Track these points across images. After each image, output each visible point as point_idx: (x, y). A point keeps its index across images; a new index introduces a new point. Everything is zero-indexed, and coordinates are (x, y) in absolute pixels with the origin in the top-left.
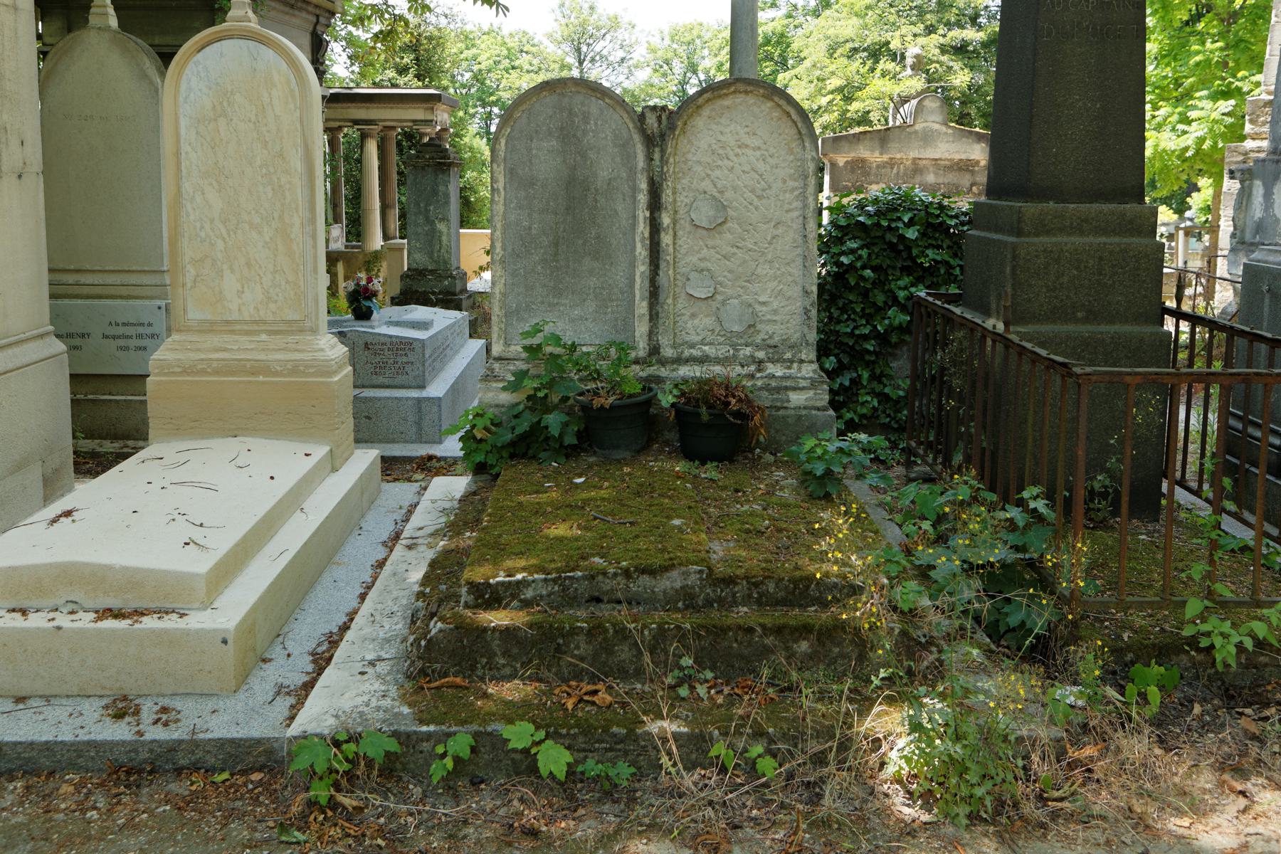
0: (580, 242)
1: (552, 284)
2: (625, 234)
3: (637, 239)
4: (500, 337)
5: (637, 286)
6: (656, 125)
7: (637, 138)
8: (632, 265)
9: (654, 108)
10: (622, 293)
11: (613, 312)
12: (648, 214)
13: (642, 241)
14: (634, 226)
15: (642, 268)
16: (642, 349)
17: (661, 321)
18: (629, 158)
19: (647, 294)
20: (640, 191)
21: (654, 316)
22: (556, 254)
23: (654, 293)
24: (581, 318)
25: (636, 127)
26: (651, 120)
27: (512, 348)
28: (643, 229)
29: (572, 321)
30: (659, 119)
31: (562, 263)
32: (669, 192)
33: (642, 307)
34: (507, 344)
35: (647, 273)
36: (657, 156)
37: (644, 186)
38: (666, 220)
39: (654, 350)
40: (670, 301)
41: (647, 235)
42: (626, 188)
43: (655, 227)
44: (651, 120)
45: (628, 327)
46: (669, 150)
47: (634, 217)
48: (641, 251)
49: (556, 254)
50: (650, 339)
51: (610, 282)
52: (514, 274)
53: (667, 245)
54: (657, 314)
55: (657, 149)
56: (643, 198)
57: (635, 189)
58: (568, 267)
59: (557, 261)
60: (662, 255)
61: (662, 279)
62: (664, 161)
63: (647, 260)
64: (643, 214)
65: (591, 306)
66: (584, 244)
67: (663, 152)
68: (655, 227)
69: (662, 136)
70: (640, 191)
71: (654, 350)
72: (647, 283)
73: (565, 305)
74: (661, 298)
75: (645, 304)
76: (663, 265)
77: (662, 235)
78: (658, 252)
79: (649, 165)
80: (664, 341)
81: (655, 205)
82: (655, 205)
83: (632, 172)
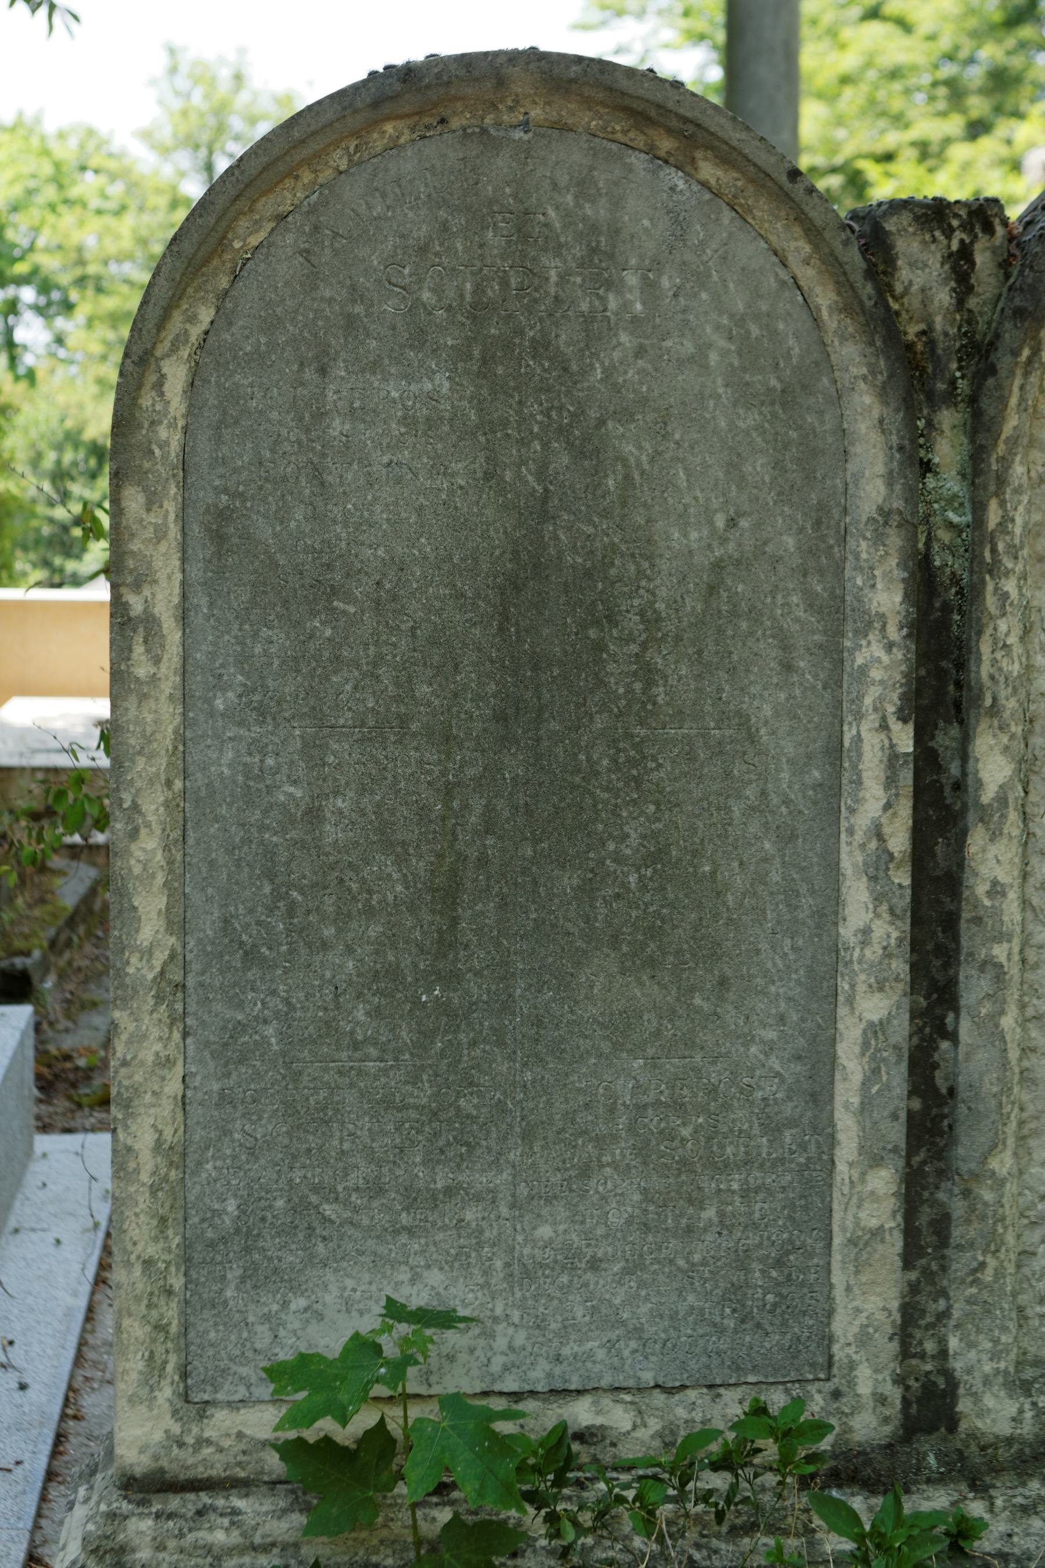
0: (569, 881)
1: (424, 1095)
2: (787, 837)
3: (851, 860)
4: (154, 1367)
5: (847, 1092)
6: (943, 297)
7: (852, 356)
8: (824, 992)
9: (935, 214)
10: (773, 1129)
11: (725, 1224)
12: (905, 740)
13: (877, 868)
14: (832, 796)
15: (873, 1007)
16: (865, 1406)
17: (960, 1264)
18: (810, 460)
19: (897, 1134)
20: (869, 623)
21: (926, 1237)
22: (446, 943)
23: (932, 1125)
24: (569, 1260)
25: (850, 306)
26: (921, 270)
27: (221, 1423)
28: (877, 809)
29: (523, 1274)
30: (960, 265)
31: (474, 988)
32: (1007, 627)
33: (868, 1197)
34: (193, 1404)
35: (901, 1030)
36: (948, 450)
37: (888, 598)
38: (993, 768)
39: (930, 1405)
40: (1002, 1163)
41: (899, 841)
42: (795, 612)
43: (940, 806)
44: (921, 270)
45: (790, 1291)
46: (1011, 422)
47: (836, 754)
48: (869, 922)
49: (446, 943)
50: (905, 1354)
51: (716, 1074)
52: (231, 1049)
53: (997, 890)
54: (942, 1225)
55: (948, 418)
56: (881, 662)
57: (838, 616)
58: (507, 1007)
59: (452, 979)
60: (968, 937)
61: (971, 1058)
62: (980, 471)
63: (900, 967)
64: (879, 738)
65: (619, 1197)
66: (587, 890)
67: (980, 428)
68: (940, 806)
69: (981, 354)
70: (869, 623)
71: (930, 1405)
72: (896, 1078)
73: (489, 1197)
74: (965, 1151)
75: (884, 1181)
76: (974, 986)
77: (977, 840)
78: (950, 923)
79: (915, 495)
80: (975, 1358)
81: (942, 689)
82: (942, 689)
83: (827, 528)
